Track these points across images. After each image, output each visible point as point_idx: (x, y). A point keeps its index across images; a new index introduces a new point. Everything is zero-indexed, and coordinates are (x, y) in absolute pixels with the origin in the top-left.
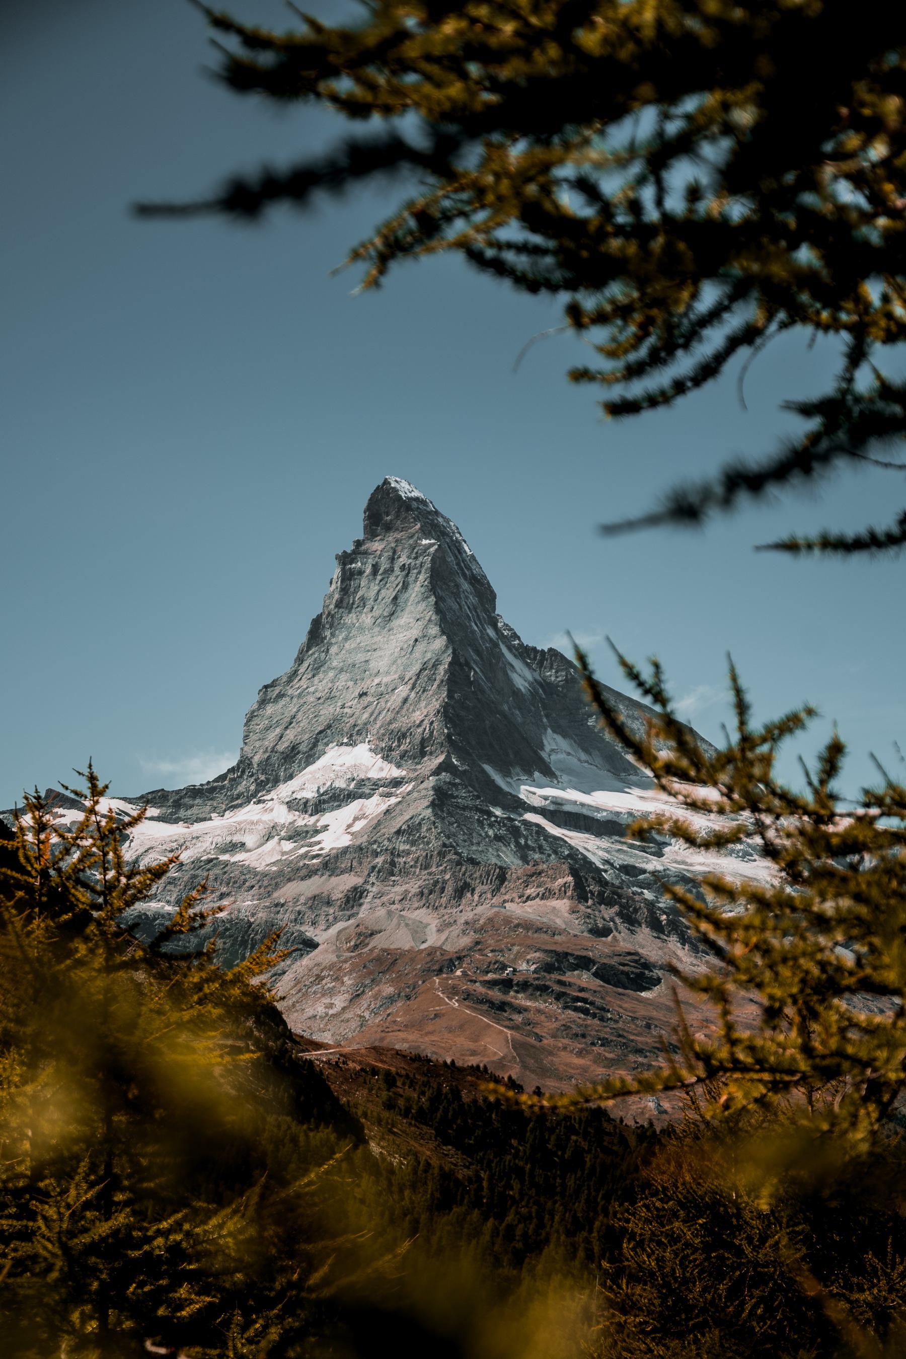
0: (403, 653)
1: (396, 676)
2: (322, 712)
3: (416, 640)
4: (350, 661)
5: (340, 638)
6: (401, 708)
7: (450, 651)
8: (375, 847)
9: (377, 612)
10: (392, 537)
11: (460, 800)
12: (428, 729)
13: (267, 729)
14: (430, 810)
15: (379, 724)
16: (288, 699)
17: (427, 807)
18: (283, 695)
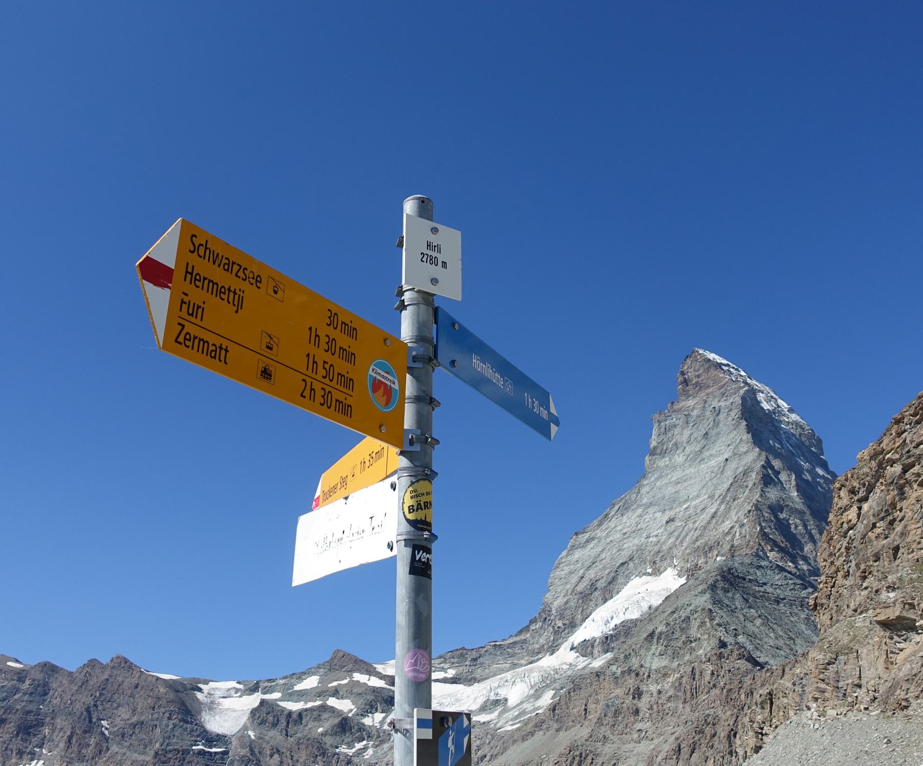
0: (713, 475)
1: (706, 497)
2: (626, 546)
3: (727, 460)
4: (660, 495)
5: (652, 479)
6: (709, 523)
7: (763, 457)
8: (614, 668)
9: (688, 449)
10: (702, 394)
11: (770, 590)
12: (738, 534)
13: (571, 573)
14: (708, 596)
15: (685, 544)
16: (596, 541)
17: (703, 592)
18: (593, 539)
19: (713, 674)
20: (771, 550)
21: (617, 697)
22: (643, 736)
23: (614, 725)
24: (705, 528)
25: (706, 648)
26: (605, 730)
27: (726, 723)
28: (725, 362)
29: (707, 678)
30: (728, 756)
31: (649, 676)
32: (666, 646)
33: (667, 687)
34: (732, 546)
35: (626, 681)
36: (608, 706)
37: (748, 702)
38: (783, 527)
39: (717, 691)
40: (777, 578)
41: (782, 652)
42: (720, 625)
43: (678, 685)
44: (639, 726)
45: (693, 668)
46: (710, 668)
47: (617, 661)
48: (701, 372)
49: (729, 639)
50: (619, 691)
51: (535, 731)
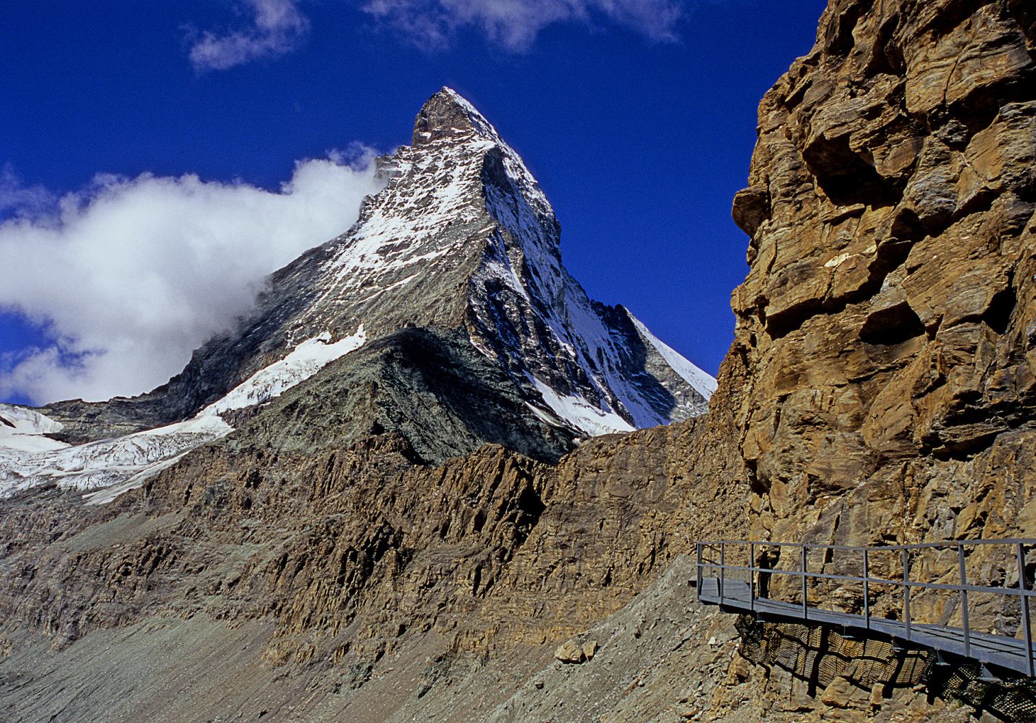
8: (233, 444)
12: (441, 309)
14: (379, 367)
15: (377, 314)
19: (354, 466)
20: (476, 334)
21: (226, 482)
22: (247, 536)
23: (214, 518)
24: (405, 297)
25: (358, 430)
26: (201, 522)
27: (348, 537)
28: (477, 113)
29: (346, 472)
30: (336, 585)
31: (275, 460)
32: (307, 424)
33: (294, 476)
34: (431, 323)
35: (244, 462)
36: (212, 491)
37: (385, 512)
38: (496, 309)
39: (352, 490)
40: (473, 361)
41: (456, 452)
42: (380, 404)
43: (309, 478)
44: (246, 522)
45: (333, 456)
46: (352, 458)
47: (239, 436)
48: (445, 117)
49: (389, 425)
50: (232, 475)
51: (120, 511)
